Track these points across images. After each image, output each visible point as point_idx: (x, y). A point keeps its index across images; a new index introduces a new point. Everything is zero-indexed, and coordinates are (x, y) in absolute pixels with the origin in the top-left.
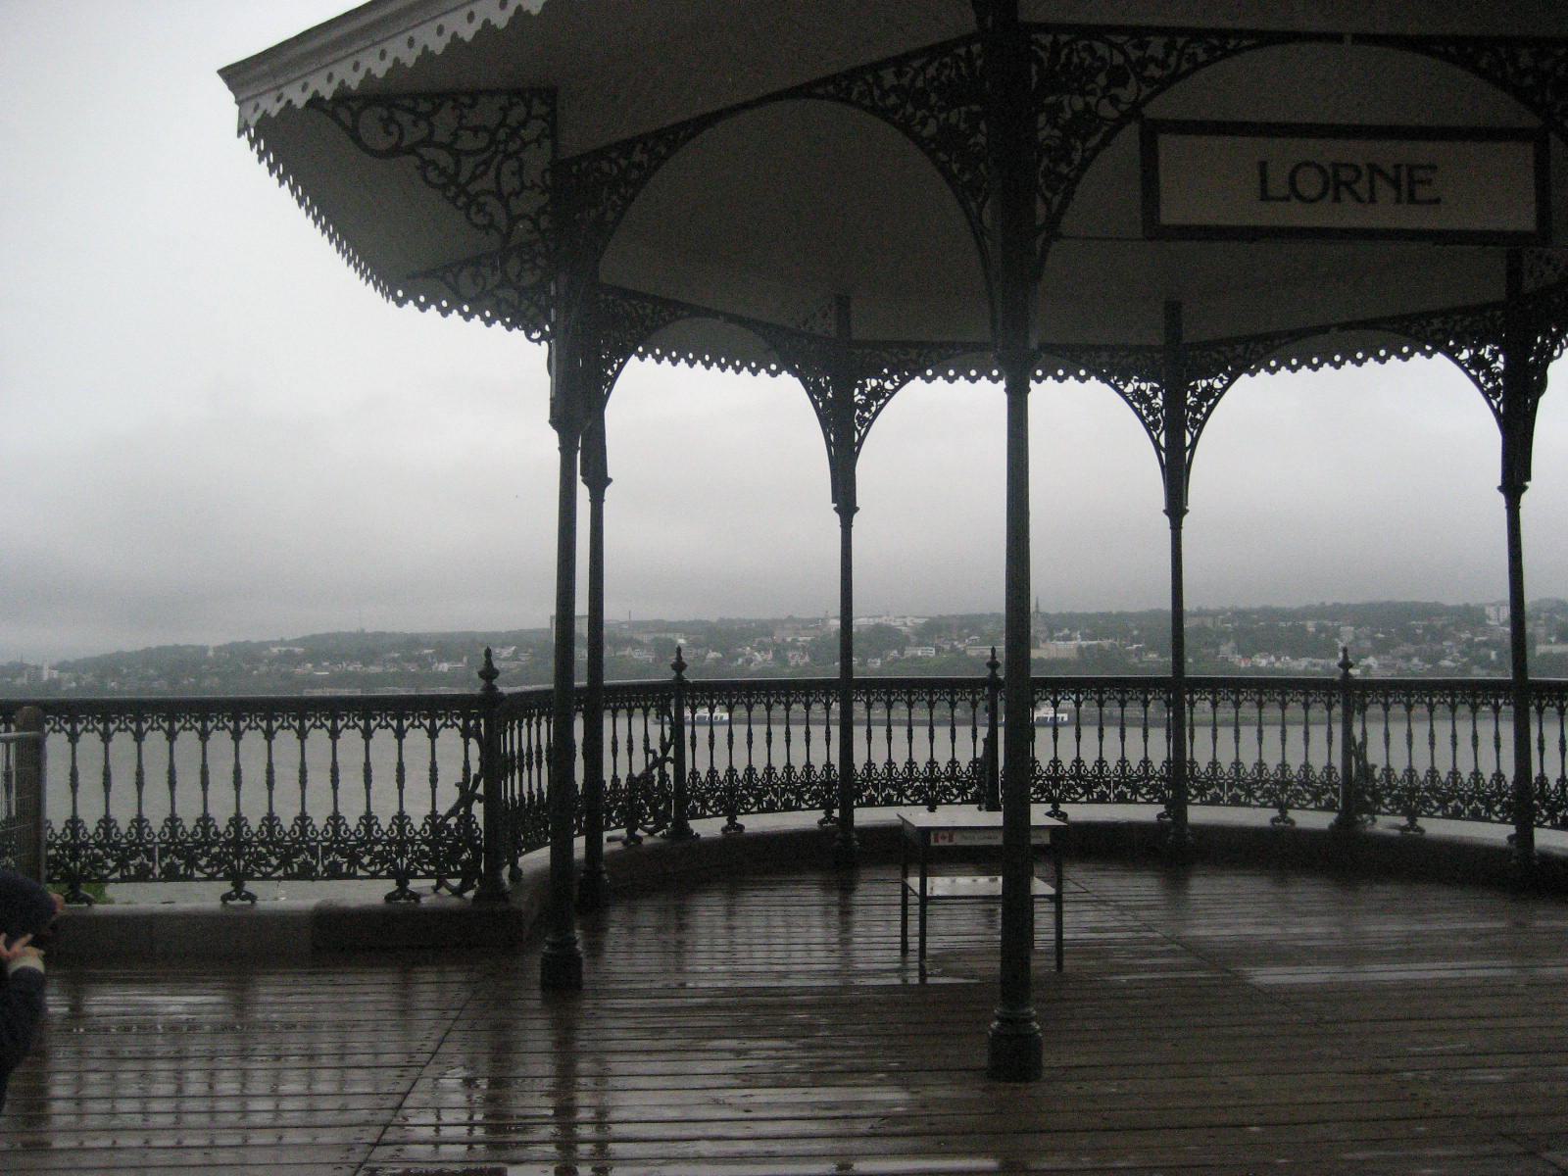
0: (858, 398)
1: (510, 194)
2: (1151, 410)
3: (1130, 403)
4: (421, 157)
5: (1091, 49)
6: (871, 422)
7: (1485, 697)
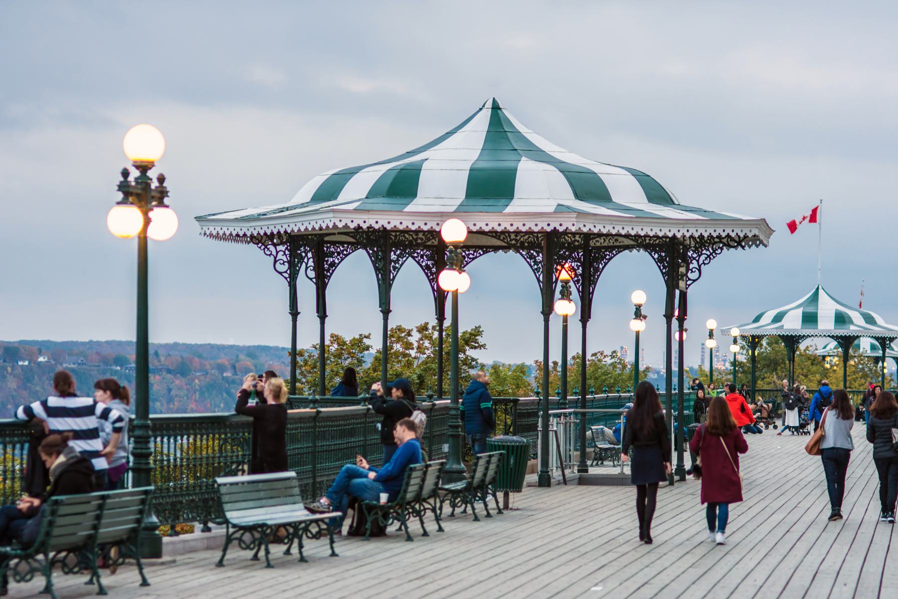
5: (404, 236)
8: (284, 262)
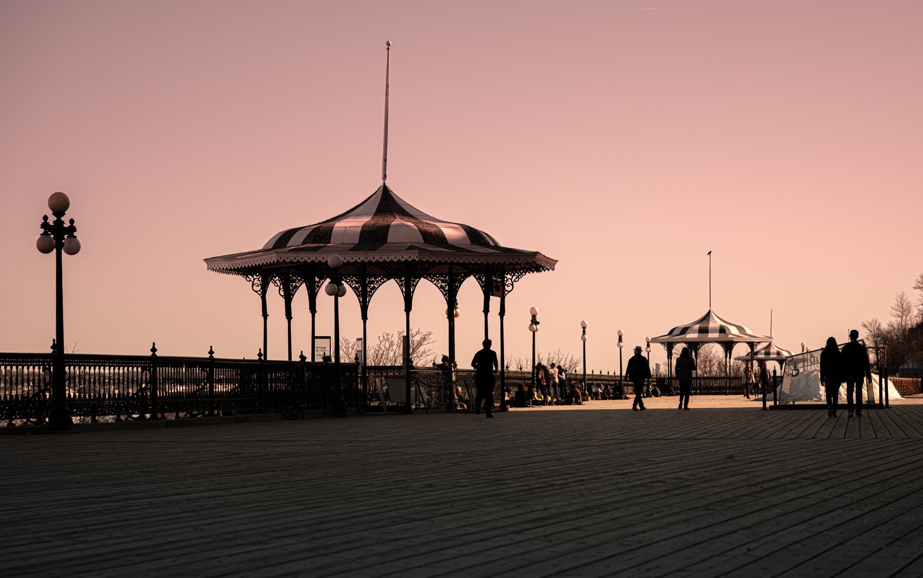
0: (368, 290)
2: (445, 291)
3: (439, 289)
8: (258, 285)
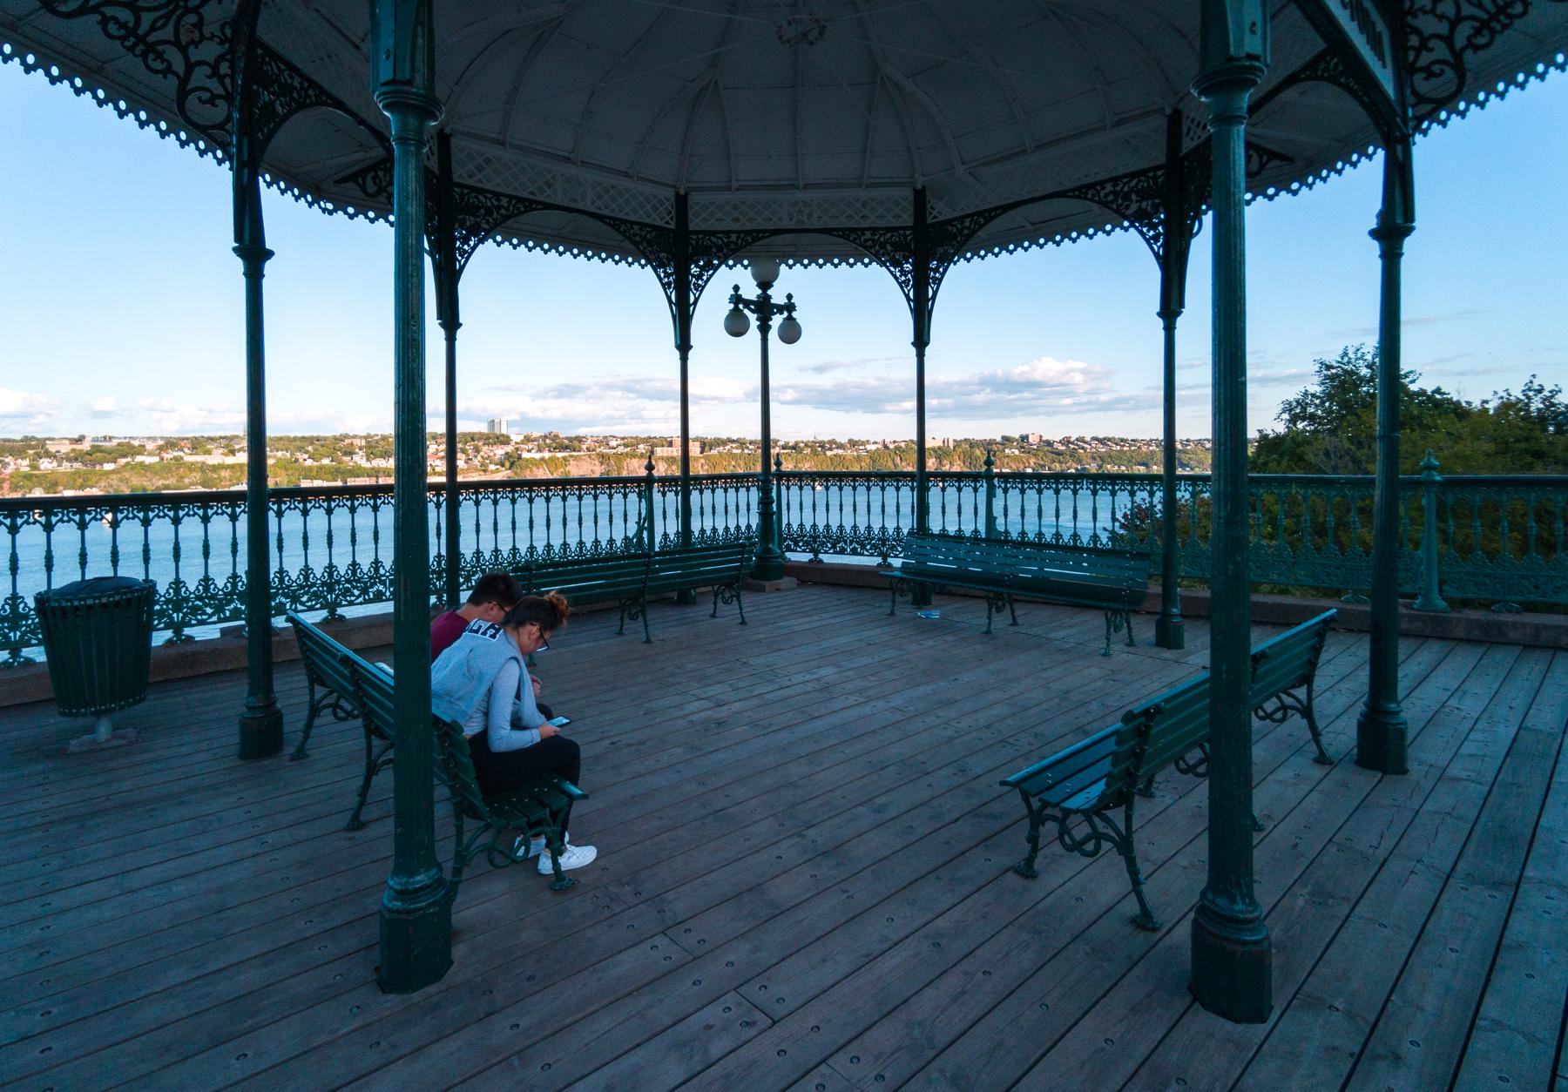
1: (188, 44)
2: (903, 273)
4: (102, 14)
6: (703, 287)
7: (1048, 484)
